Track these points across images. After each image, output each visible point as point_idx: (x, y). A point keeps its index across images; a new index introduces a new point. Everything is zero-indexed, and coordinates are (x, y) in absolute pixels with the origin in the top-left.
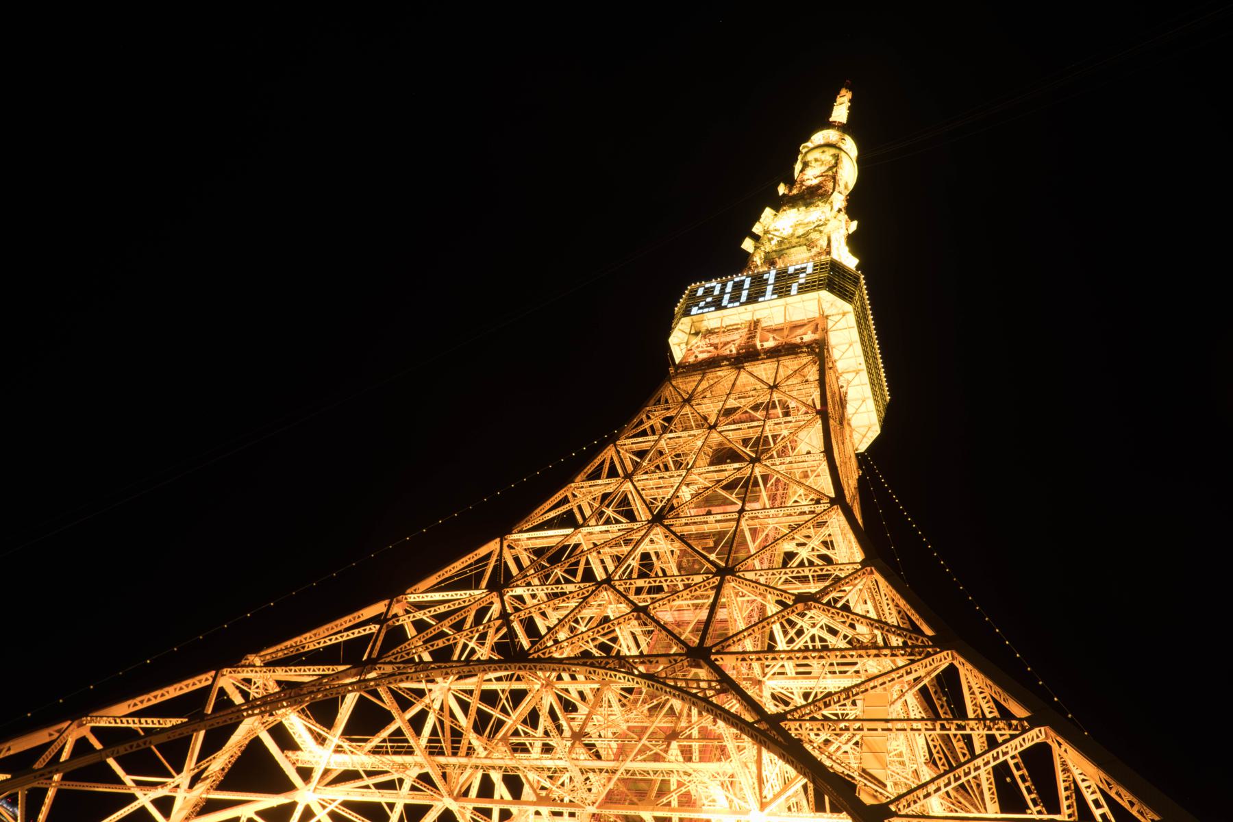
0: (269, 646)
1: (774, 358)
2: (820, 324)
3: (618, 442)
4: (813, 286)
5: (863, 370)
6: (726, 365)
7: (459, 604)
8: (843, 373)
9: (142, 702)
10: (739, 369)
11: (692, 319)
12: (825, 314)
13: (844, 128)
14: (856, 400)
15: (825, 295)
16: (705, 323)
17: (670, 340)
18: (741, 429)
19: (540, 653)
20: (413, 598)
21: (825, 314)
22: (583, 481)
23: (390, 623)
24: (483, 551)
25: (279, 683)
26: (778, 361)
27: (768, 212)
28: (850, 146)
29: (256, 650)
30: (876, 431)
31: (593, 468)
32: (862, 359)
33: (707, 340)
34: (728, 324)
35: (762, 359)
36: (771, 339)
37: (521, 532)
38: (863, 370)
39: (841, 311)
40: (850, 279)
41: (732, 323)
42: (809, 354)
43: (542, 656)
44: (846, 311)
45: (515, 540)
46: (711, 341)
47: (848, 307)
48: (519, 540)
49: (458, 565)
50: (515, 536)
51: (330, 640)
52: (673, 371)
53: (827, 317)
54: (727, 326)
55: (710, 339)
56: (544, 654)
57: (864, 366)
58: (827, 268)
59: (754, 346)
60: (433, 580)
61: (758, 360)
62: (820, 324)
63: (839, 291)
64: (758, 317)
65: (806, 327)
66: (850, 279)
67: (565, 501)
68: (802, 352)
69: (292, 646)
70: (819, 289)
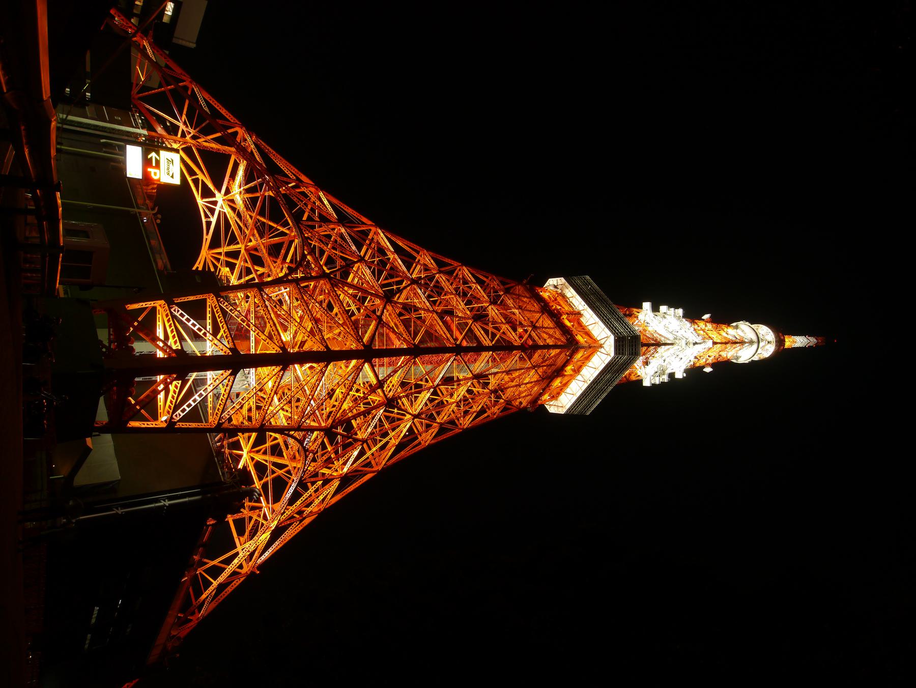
0: (265, 142)
1: (556, 325)
2: (594, 346)
3: (464, 268)
4: (615, 331)
5: (587, 383)
6: (541, 305)
7: (324, 209)
8: (581, 375)
9: (218, 106)
10: (542, 311)
11: (565, 283)
12: (603, 346)
13: (780, 342)
14: (571, 390)
15: (612, 337)
16: (567, 291)
17: (550, 279)
18: (498, 316)
19: (304, 229)
20: (321, 194)
21: (603, 346)
22: (429, 255)
23: (300, 184)
24: (364, 220)
25: (252, 151)
26: (556, 328)
27: (680, 312)
28: (767, 350)
29: (257, 136)
30: (562, 411)
31: (442, 259)
32: (592, 379)
33: (557, 295)
34: (573, 302)
35: (553, 320)
36: (572, 324)
37: (383, 233)
38: (587, 383)
39: (609, 353)
40: (632, 350)
41: (574, 304)
42: (567, 340)
43: (303, 230)
44: (611, 354)
45: (379, 233)
46: (558, 298)
47: (612, 354)
48: (380, 234)
49: (349, 211)
50: (380, 231)
51: (287, 171)
52: (524, 282)
53: (603, 347)
54: (571, 302)
55: (558, 296)
56: (305, 231)
57: (589, 382)
58: (632, 334)
59: (561, 315)
60: (335, 201)
61: (551, 318)
62: (594, 346)
63: (619, 346)
64: (584, 314)
65: (592, 340)
66: (632, 350)
67: (418, 252)
68: (566, 336)
69: (270, 152)
70: (614, 334)
